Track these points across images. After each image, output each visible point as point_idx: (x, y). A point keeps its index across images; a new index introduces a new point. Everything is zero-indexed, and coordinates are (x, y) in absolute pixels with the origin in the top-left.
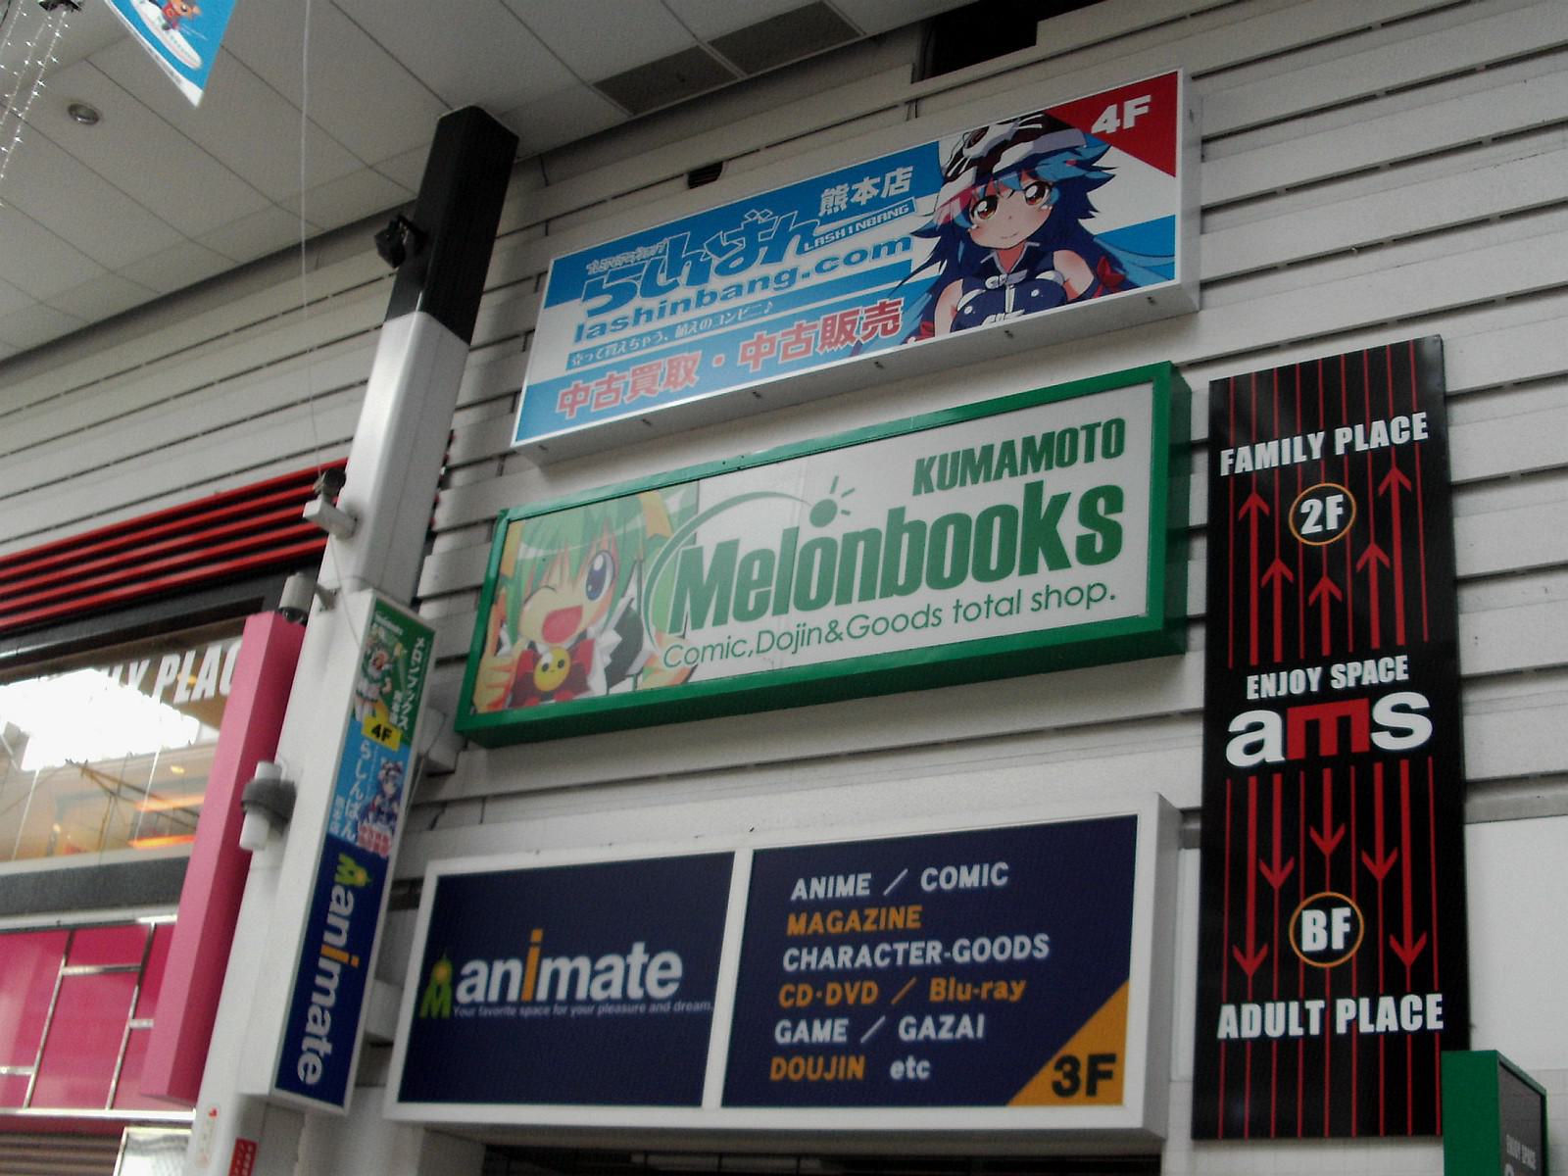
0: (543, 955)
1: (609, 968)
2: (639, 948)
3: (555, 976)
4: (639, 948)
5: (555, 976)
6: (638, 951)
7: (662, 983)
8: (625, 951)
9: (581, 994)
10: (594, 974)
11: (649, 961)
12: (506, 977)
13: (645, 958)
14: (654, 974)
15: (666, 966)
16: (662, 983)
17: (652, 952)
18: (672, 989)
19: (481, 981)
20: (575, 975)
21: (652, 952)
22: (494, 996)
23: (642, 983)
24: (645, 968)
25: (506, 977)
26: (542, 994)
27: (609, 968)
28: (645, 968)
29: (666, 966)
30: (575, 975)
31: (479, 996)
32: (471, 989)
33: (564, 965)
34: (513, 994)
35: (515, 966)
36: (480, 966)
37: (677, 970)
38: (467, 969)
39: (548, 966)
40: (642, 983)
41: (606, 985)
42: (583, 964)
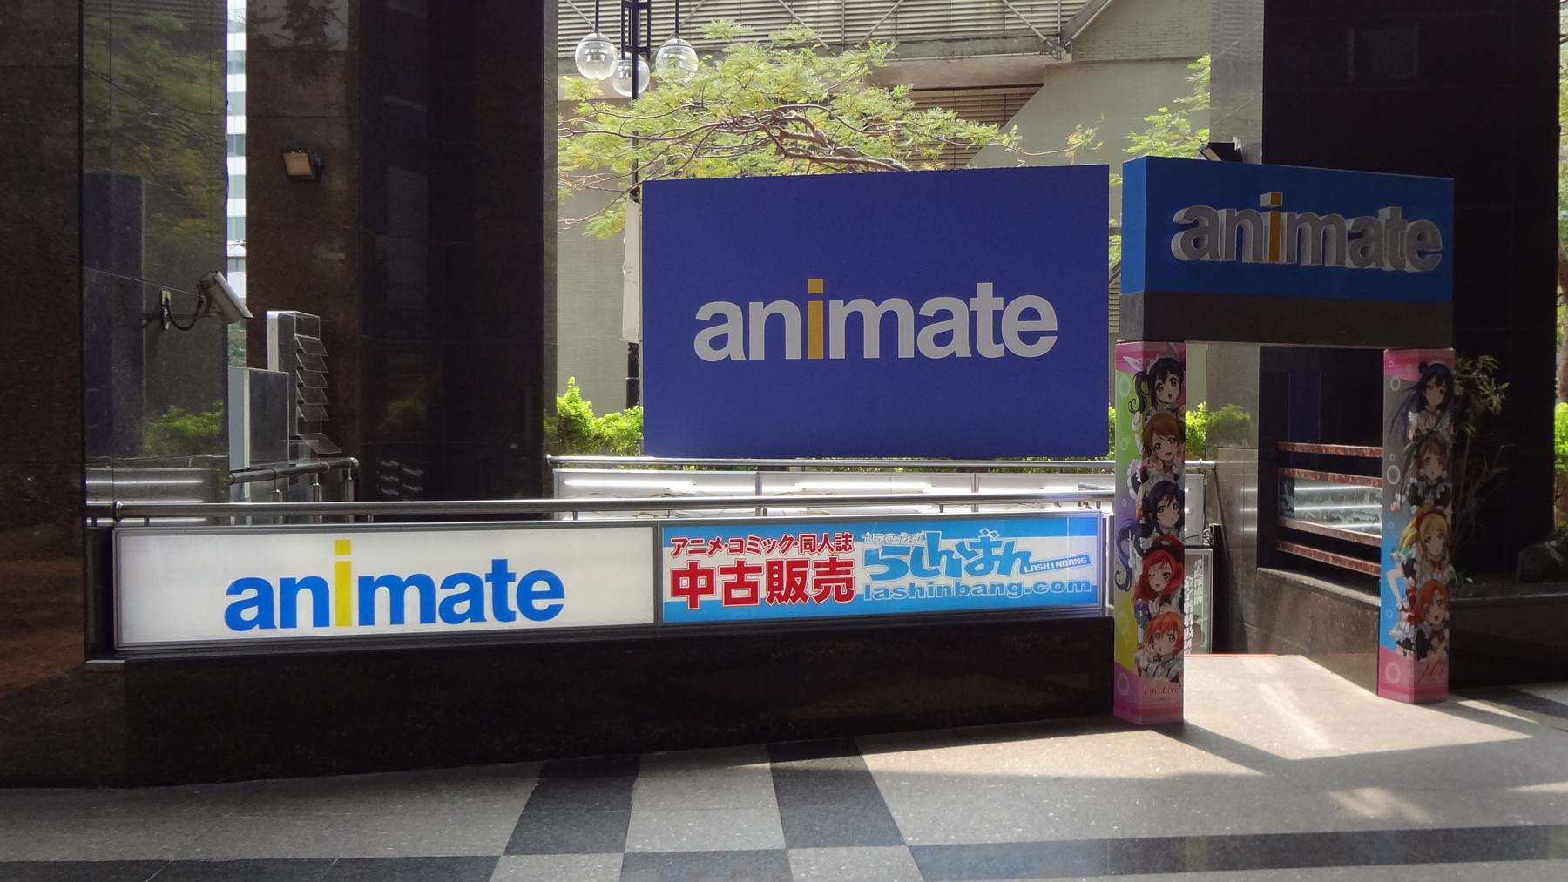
0: (826, 298)
1: (944, 315)
2: (985, 289)
3: (855, 324)
4: (985, 289)
5: (855, 324)
6: (985, 297)
7: (1029, 338)
8: (967, 293)
9: (905, 351)
10: (921, 322)
11: (1005, 306)
12: (775, 325)
13: (998, 303)
14: (1012, 326)
15: (1030, 314)
16: (1029, 338)
17: (1007, 292)
18: (1045, 345)
19: (733, 329)
20: (889, 323)
21: (1007, 292)
22: (758, 352)
23: (998, 338)
24: (998, 316)
25: (775, 325)
26: (838, 351)
27: (944, 315)
28: (998, 316)
29: (1030, 314)
30: (889, 323)
31: (734, 351)
32: (719, 342)
33: (871, 312)
34: (793, 351)
35: (788, 309)
36: (730, 309)
37: (1049, 319)
38: (705, 313)
39: (839, 311)
40: (998, 338)
41: (943, 339)
42: (901, 307)
